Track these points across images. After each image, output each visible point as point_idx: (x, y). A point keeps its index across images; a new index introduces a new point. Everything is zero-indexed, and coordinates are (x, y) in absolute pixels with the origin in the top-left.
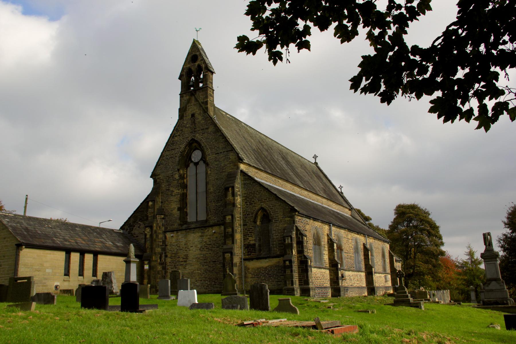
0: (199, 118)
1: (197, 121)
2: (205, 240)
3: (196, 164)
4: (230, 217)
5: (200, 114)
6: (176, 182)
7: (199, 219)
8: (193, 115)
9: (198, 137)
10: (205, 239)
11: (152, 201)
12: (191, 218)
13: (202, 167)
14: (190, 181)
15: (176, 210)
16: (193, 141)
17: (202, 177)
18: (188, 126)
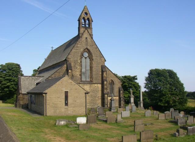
0: (89, 39)
1: (88, 41)
2: (91, 89)
3: (86, 58)
4: (106, 82)
5: (89, 38)
6: (79, 63)
7: (87, 80)
8: (86, 38)
9: (89, 48)
10: (91, 88)
11: (71, 70)
12: (84, 79)
13: (88, 60)
14: (84, 64)
15: (79, 75)
16: (87, 48)
17: (88, 64)
18: (84, 42)
